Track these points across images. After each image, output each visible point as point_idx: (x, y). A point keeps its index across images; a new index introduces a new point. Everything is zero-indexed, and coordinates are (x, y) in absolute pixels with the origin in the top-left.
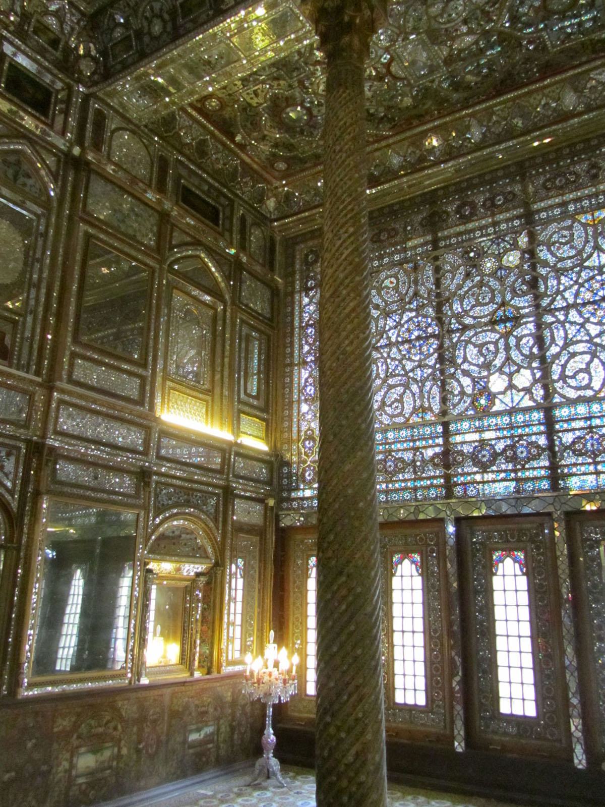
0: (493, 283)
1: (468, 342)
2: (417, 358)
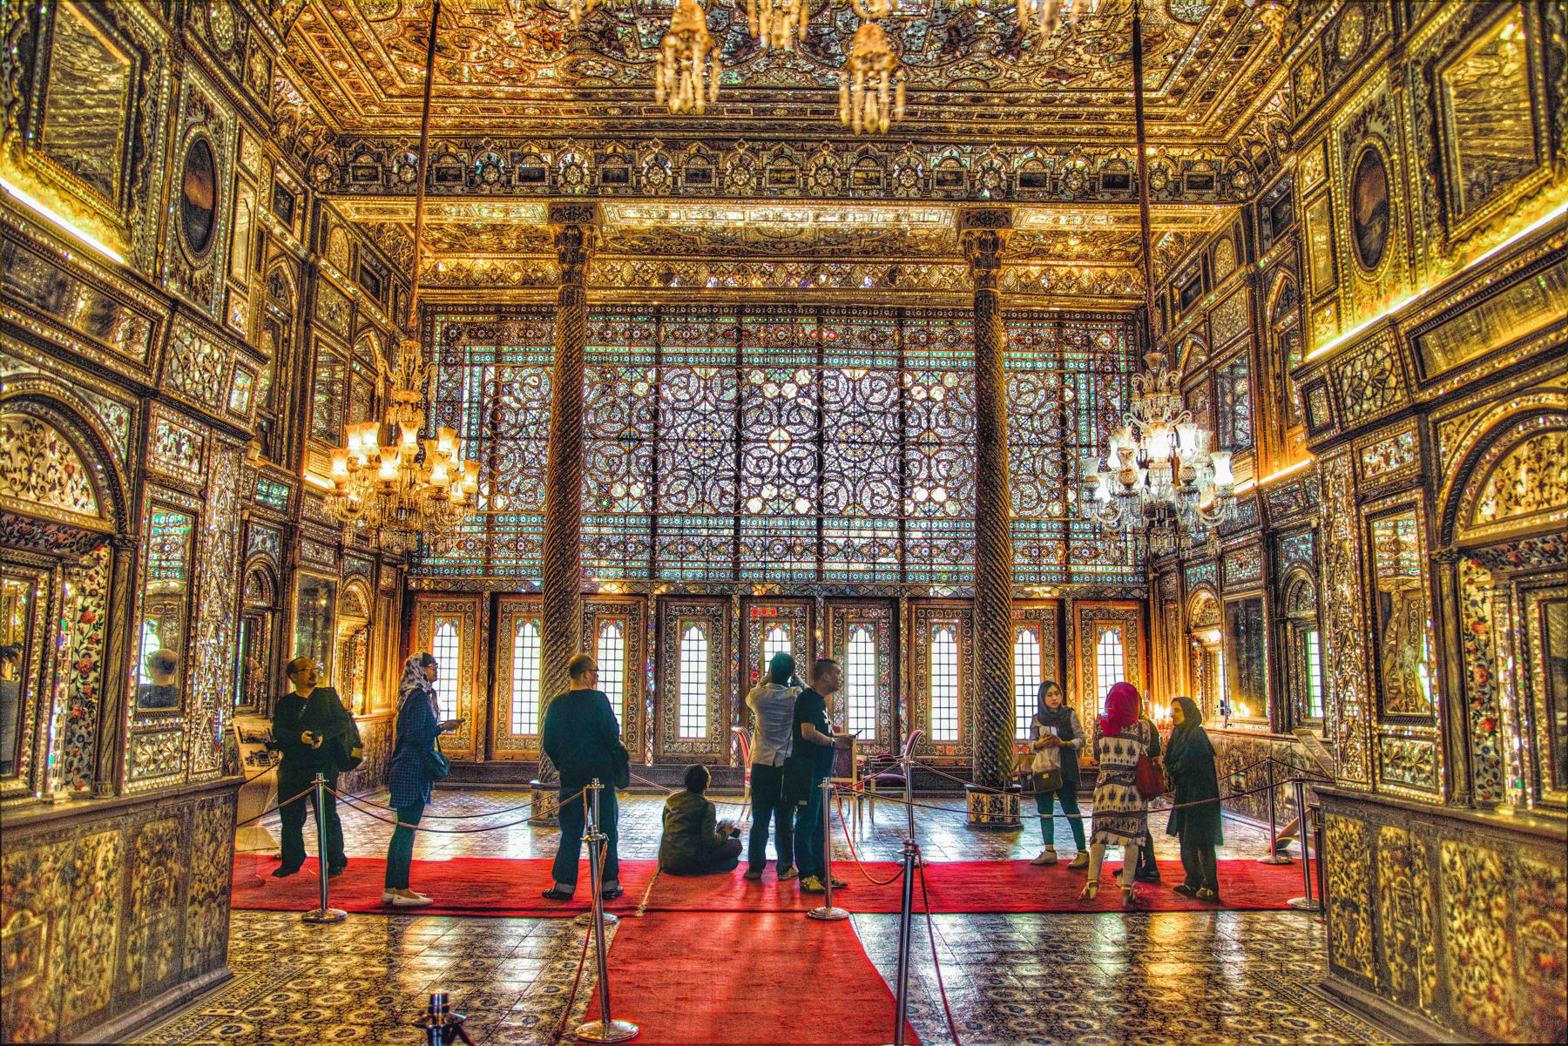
0: (624, 405)
1: (598, 451)
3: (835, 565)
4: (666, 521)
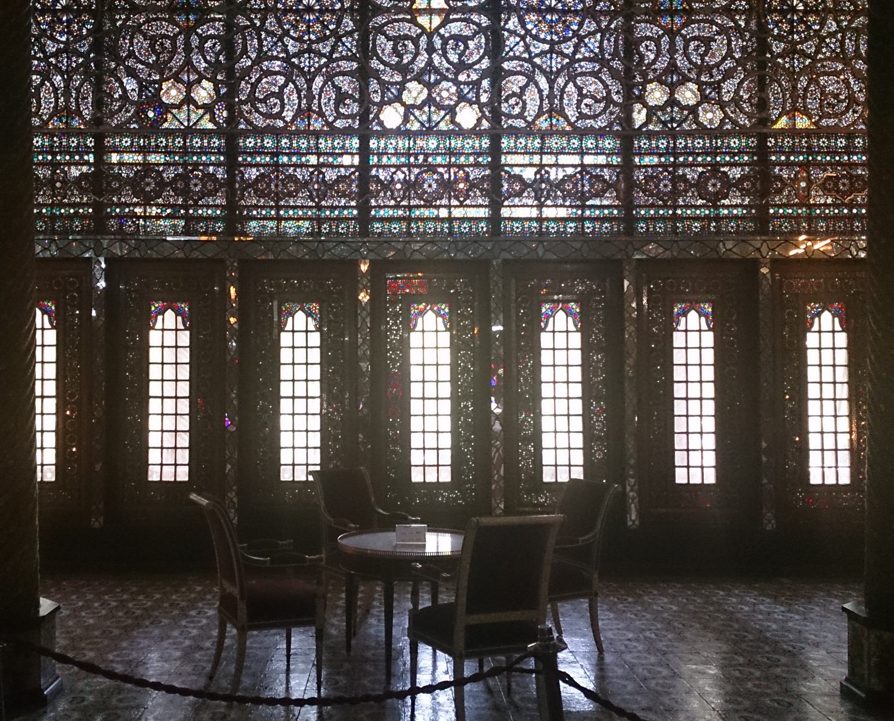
1: (138, 28)
2: (64, 39)
4: (250, 142)
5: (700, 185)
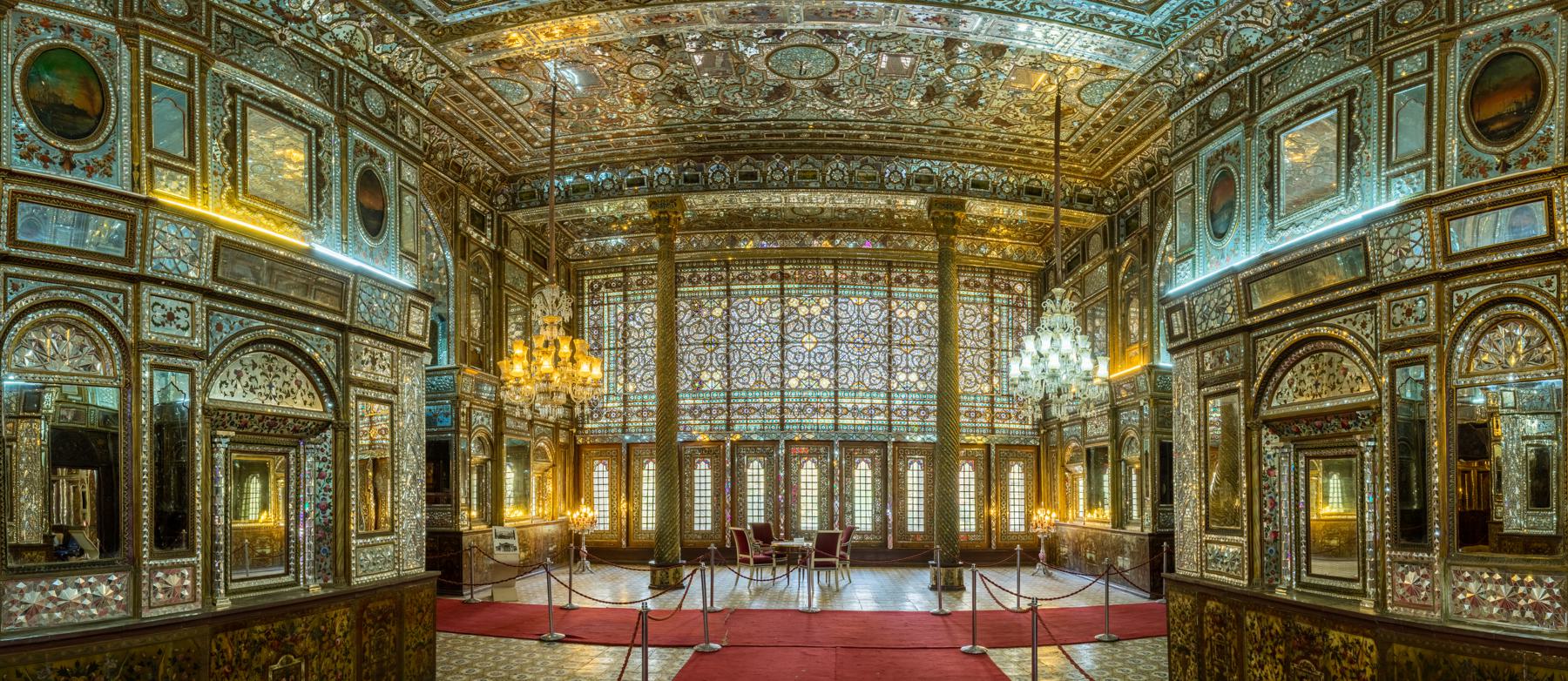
3: (846, 421)
5: (918, 412)
